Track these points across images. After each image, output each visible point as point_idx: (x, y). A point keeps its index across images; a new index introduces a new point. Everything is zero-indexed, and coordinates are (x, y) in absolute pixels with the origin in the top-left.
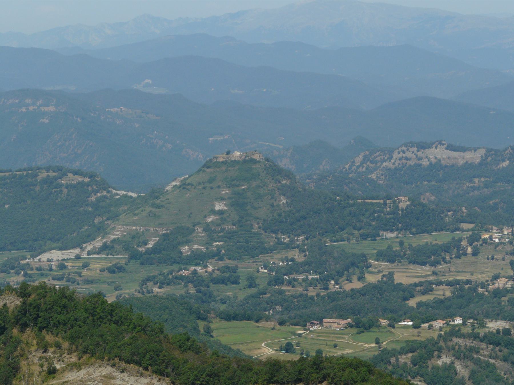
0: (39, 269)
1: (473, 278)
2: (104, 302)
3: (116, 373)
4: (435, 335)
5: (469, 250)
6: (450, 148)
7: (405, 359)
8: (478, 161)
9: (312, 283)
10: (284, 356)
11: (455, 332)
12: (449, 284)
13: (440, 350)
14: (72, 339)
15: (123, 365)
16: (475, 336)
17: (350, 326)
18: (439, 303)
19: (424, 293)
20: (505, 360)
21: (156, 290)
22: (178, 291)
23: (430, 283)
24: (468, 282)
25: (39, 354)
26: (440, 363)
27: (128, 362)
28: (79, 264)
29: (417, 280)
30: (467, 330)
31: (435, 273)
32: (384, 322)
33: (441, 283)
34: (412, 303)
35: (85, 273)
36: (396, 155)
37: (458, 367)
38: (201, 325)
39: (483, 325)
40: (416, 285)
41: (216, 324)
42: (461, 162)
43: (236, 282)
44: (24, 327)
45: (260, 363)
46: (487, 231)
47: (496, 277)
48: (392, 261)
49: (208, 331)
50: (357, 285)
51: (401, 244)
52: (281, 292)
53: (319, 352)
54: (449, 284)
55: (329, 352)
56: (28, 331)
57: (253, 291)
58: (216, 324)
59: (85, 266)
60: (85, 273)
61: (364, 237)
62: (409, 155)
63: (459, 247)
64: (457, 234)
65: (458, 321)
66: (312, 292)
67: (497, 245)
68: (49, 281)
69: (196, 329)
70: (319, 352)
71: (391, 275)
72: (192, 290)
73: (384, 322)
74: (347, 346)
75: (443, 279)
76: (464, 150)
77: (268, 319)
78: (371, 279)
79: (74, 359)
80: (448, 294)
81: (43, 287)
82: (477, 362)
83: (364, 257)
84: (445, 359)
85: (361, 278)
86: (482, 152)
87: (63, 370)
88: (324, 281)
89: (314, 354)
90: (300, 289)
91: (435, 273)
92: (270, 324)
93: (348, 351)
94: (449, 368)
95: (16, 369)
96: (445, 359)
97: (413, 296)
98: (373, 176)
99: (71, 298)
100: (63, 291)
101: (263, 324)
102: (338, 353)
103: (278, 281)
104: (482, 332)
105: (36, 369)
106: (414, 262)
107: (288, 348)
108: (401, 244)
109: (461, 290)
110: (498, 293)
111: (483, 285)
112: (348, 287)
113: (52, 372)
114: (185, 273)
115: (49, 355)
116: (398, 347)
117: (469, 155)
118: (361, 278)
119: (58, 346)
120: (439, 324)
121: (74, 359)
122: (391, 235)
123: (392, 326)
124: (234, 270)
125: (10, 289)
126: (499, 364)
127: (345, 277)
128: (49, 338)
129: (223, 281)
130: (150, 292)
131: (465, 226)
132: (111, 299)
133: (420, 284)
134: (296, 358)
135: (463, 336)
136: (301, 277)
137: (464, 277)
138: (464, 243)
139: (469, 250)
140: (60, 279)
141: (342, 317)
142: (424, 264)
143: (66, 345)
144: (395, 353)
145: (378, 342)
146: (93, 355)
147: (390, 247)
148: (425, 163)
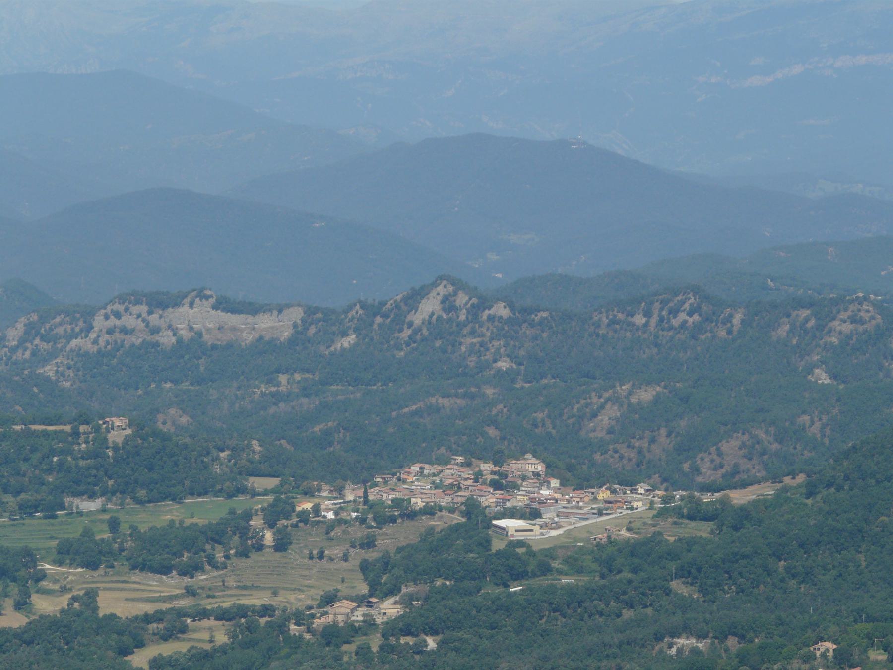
1: (278, 601)
5: (269, 537)
6: (224, 305)
8: (286, 334)
12: (223, 616)
19: (166, 637)
23: (181, 614)
24: (267, 610)
29: (149, 608)
31: (190, 592)
33: (204, 614)
36: (99, 322)
40: (148, 619)
42: (248, 338)
46: (308, 493)
47: (329, 600)
48: (92, 565)
51: (114, 525)
54: (223, 616)
61: (27, 509)
62: (129, 321)
63: (243, 531)
64: (241, 502)
67: (331, 526)
71: (91, 596)
75: (209, 604)
76: (254, 309)
80: (222, 638)
83: (29, 557)
85: (22, 605)
86: (296, 314)
91: (190, 592)
97: (140, 645)
98: (49, 370)
106: (144, 567)
108: (114, 525)
109: (250, 628)
111: (299, 618)
117: (265, 322)
118: (22, 605)
122: (90, 506)
127: (404, 585)
131: (259, 483)
133: (158, 617)
137: (257, 600)
138: (256, 522)
139: (269, 537)
142: (164, 570)
147: (87, 533)
148: (167, 339)
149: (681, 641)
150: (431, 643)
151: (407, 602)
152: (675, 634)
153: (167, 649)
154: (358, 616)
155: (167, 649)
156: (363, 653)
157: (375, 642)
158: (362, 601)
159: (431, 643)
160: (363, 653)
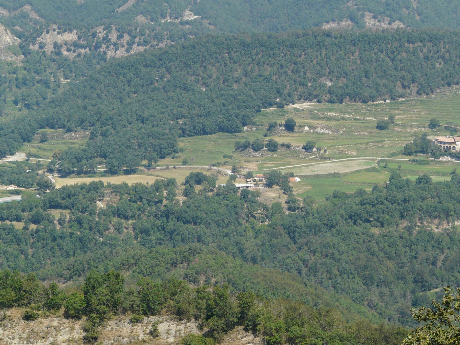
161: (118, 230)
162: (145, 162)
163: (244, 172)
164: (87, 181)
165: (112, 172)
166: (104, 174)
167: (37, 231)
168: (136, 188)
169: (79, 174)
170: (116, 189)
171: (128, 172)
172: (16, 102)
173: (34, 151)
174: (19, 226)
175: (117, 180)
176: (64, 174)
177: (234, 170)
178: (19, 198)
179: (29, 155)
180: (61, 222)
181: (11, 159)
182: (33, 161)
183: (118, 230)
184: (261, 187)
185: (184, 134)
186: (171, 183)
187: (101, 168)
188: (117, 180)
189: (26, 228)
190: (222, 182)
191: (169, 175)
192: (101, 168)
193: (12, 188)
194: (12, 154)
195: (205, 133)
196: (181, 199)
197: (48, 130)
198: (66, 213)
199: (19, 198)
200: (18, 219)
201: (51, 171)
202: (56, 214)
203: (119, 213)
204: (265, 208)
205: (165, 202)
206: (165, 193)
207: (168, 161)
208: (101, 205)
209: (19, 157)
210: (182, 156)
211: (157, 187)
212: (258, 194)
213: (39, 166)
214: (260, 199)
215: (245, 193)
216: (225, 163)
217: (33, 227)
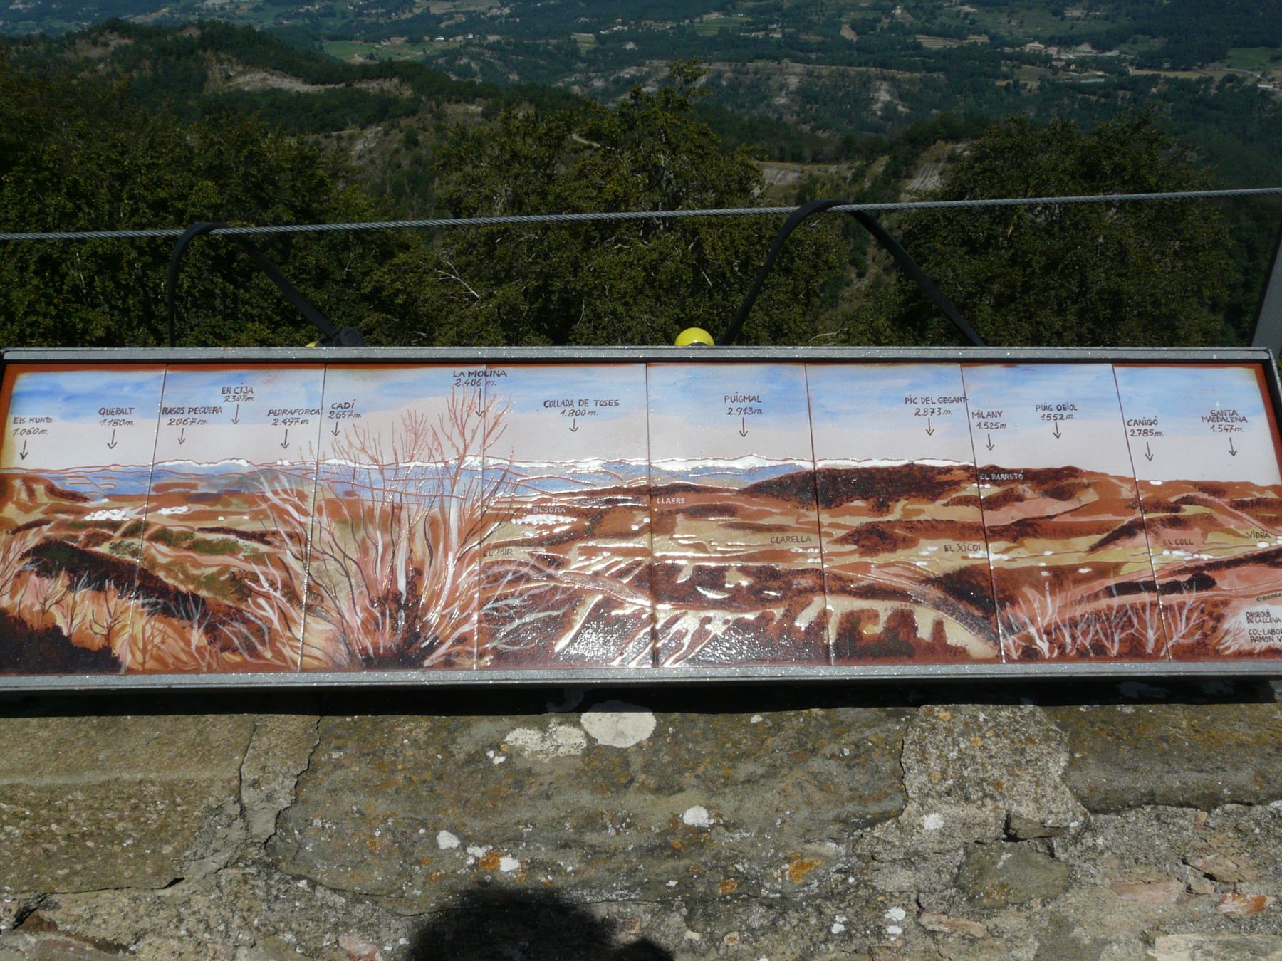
0: (208, 10)
1: (477, 9)
2: (254, 31)
3: (269, 77)
4: (458, 46)
7: (441, 61)
9: (382, 15)
10: (369, 62)
11: (469, 43)
12: (463, 13)
13: (461, 54)
14: (238, 56)
15: (272, 71)
16: (481, 46)
17: (406, 41)
18: (458, 25)
19: (448, 20)
20: (499, 59)
21: (285, 22)
22: (299, 22)
23: (452, 13)
24: (474, 12)
25: (218, 66)
26: (462, 62)
27: (275, 69)
28: (233, 6)
29: (443, 11)
30: (476, 42)
31: (454, 6)
32: (427, 38)
33: (458, 13)
34: (443, 25)
35: (237, 12)
37: (473, 65)
38: (317, 44)
39: (485, 38)
40: (444, 14)
41: (325, 43)
43: (334, 15)
44: (205, 50)
45: (354, 66)
47: (491, 8)
49: (321, 48)
50: (409, 15)
52: (363, 21)
53: (390, 59)
54: (463, 13)
55: (395, 58)
56: (209, 51)
57: (345, 21)
58: (325, 43)
59: (237, 7)
60: (237, 12)
65: (471, 36)
66: (382, 21)
68: (216, 18)
69: (313, 46)
70: (390, 59)
71: (428, 9)
72: (308, 22)
73: (427, 38)
74: (407, 54)
75: (459, 10)
77: (357, 39)
78: (417, 11)
79: (240, 68)
80: (464, 20)
81: (213, 22)
82: (483, 61)
84: (465, 61)
85: (411, 11)
87: (235, 76)
88: (388, 14)
89: (386, 60)
90: (374, 19)
91: (454, 6)
92: (359, 42)
93: (407, 58)
94: (468, 65)
95: (206, 77)
96: (465, 61)
97: (442, 21)
99: (232, 28)
100: (227, 24)
101: (353, 42)
102: (402, 59)
103: (360, 14)
104: (485, 43)
105: (218, 76)
107: (371, 57)
110: (493, 18)
111: (484, 13)
112: (403, 17)
113: (229, 78)
114: (302, 10)
115: (225, 66)
116: (436, 54)
118: (411, 11)
119: (229, 60)
120: (459, 38)
121: (240, 68)
123: (432, 40)
124: (332, 8)
125: (192, 24)
126: (497, 62)
128: (223, 56)
129: (324, 15)
130: (282, 24)
132: (258, 29)
133: (446, 14)
134: (377, 62)
135: (475, 46)
136: (374, 12)
137: (472, 9)
140: (222, 17)
141: (402, 36)
143: (234, 60)
144: (434, 57)
145: (424, 51)
146: (252, 65)
149: (582, 19)
150: (518, 20)
151: (511, 9)
152: (580, 16)
153: (450, 23)
154: (498, 13)
155: (450, 23)
156: (500, 23)
157: (503, 21)
158: (499, 8)
159: (518, 20)
160: (500, 23)
161: (1160, 108)
162: (1199, 64)
163: (1269, 77)
164: (1150, 73)
165: (1173, 69)
166: (1167, 70)
167: (1105, 104)
168: (1183, 81)
169: (1150, 68)
170: (1168, 80)
171: (1184, 70)
172: (1127, 15)
173: (1125, 49)
174: (1094, 98)
175: (1172, 75)
176: (1139, 67)
177: (1264, 75)
178: (1102, 80)
179: (1121, 52)
180: (1123, 99)
181: (1109, 54)
182: (1123, 55)
183: (1160, 108)
184: (1277, 89)
185: (1236, 45)
186: (1211, 80)
187: (1167, 65)
188: (1172, 75)
189: (1097, 101)
190: (1249, 83)
191: (1211, 74)
192: (1167, 65)
193: (1100, 73)
194: (1110, 51)
195: (1252, 46)
196: (1213, 91)
197: (1140, 36)
198: (1128, 94)
199: (1102, 80)
200: (1094, 94)
201: (1132, 64)
202: (1121, 93)
203: (1165, 97)
204: (1275, 104)
205: (1201, 92)
206: (1202, 87)
207: (1217, 64)
208: (1154, 90)
209: (1114, 53)
210: (1228, 61)
211: (1199, 82)
212: (1273, 93)
213: (1125, 60)
214: (1273, 98)
215: (1264, 91)
216: (1259, 69)
217: (1103, 100)
